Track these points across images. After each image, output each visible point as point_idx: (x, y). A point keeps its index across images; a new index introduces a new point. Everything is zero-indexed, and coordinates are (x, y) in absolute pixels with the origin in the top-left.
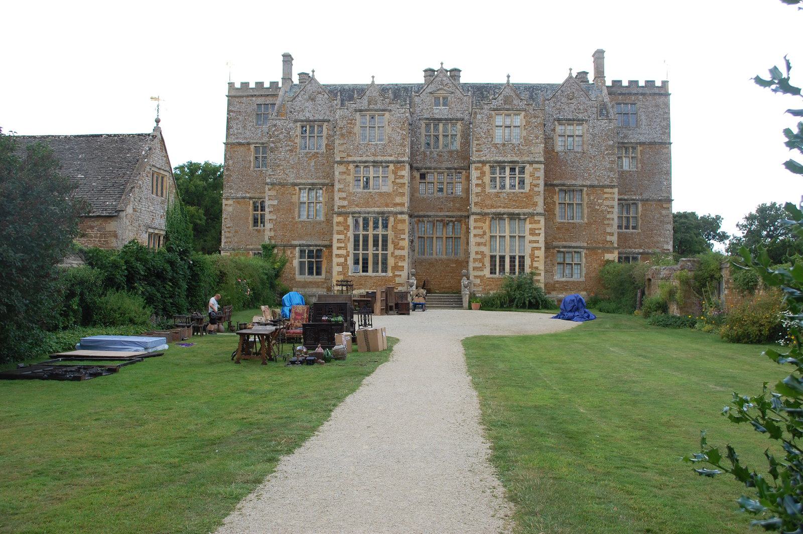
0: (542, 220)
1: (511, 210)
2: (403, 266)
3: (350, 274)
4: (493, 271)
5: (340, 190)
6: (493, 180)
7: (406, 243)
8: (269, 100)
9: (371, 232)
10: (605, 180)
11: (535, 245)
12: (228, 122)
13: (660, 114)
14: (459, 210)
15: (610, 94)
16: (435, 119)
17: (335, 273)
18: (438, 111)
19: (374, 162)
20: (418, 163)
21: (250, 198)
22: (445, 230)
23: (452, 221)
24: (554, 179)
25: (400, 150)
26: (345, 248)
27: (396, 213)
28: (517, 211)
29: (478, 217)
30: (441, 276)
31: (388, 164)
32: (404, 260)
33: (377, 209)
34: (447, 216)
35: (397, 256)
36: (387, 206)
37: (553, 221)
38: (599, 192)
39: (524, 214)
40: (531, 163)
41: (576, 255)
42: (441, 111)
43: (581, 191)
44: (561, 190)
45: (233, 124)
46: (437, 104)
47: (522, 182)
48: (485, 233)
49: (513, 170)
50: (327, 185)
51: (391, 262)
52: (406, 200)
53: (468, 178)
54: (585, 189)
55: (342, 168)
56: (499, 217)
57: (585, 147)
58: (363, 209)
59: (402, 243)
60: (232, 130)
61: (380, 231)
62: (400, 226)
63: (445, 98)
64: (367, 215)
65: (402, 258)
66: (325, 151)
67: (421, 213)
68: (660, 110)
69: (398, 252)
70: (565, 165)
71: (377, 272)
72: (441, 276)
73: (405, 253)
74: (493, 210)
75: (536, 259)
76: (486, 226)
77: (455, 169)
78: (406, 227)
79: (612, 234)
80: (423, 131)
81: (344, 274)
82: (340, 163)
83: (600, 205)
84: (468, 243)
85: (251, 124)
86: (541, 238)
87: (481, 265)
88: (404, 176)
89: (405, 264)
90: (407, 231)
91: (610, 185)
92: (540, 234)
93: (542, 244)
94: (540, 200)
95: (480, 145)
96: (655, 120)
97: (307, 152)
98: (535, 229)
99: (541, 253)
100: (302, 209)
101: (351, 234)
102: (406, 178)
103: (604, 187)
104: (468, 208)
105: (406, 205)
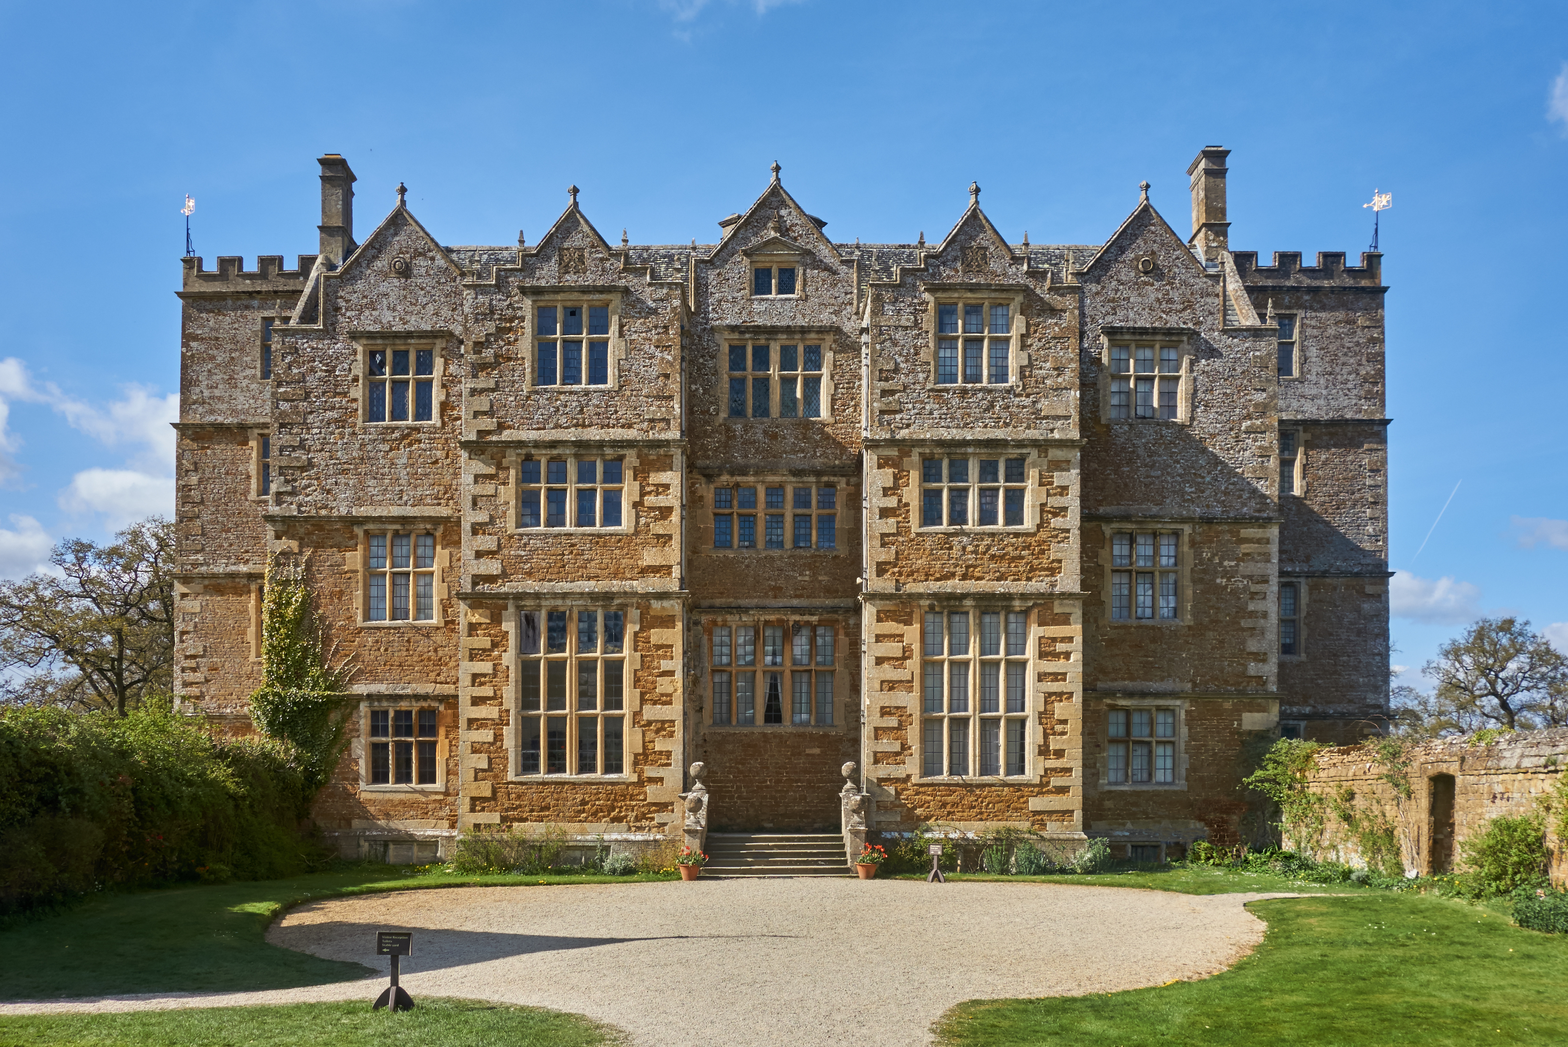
0: (1077, 613)
2: (668, 754)
3: (511, 776)
4: (930, 766)
7: (675, 686)
9: (569, 653)
10: (1244, 505)
11: (1055, 687)
12: (184, 367)
13: (1358, 344)
14: (829, 591)
16: (758, 330)
17: (466, 775)
18: (765, 305)
19: (580, 445)
20: (708, 458)
22: (787, 647)
23: (808, 623)
24: (1100, 503)
25: (655, 410)
26: (496, 698)
28: (1000, 588)
29: (889, 605)
30: (778, 781)
31: (621, 452)
32: (671, 735)
33: (588, 586)
34: (795, 610)
35: (649, 723)
37: (1096, 621)
38: (1227, 537)
39: (1023, 597)
41: (1160, 718)
43: (1176, 534)
44: (1120, 533)
45: (201, 371)
47: (1015, 500)
48: (906, 654)
49: (988, 471)
51: (631, 740)
52: (674, 554)
53: (855, 500)
54: (1187, 529)
56: (949, 605)
59: (664, 685)
60: (197, 390)
62: (657, 635)
64: (559, 602)
65: (663, 727)
66: (439, 424)
67: (718, 602)
68: (1359, 332)
69: (651, 712)
70: (1130, 462)
71: (593, 769)
72: (778, 781)
73: (675, 711)
74: (934, 586)
75: (1059, 728)
76: (912, 633)
77: (818, 473)
79: (1261, 657)
80: (724, 363)
81: (496, 776)
83: (1229, 574)
84: (856, 689)
85: (248, 372)
86: (1073, 666)
87: (897, 747)
88: (667, 487)
89: (675, 746)
90: (678, 650)
91: (1257, 519)
92: (1067, 655)
93: (1074, 684)
94: (1069, 553)
95: (892, 392)
96: (1343, 359)
97: (387, 428)
98: (1054, 640)
99: (1071, 710)
100: (374, 591)
101: (509, 658)
102: (675, 517)
104: (859, 580)
105: (676, 572)
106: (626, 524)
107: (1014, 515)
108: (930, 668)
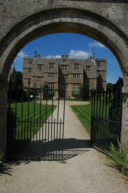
1: (77, 82)
5: (45, 78)
6: (74, 77)
8: (31, 60)
9: (51, 86)
15: (96, 61)
19: (52, 73)
21: (28, 79)
27: (56, 83)
36: (54, 81)
40: (81, 74)
42: (64, 63)
46: (64, 62)
47: (79, 77)
50: (43, 77)
52: (58, 80)
55: (46, 74)
57: (91, 71)
58: (49, 81)
61: (53, 86)
63: (65, 61)
78: (57, 85)
82: (45, 73)
94: (82, 81)
103: (94, 79)
106: (55, 78)
107: (79, 78)
108: (73, 87)
